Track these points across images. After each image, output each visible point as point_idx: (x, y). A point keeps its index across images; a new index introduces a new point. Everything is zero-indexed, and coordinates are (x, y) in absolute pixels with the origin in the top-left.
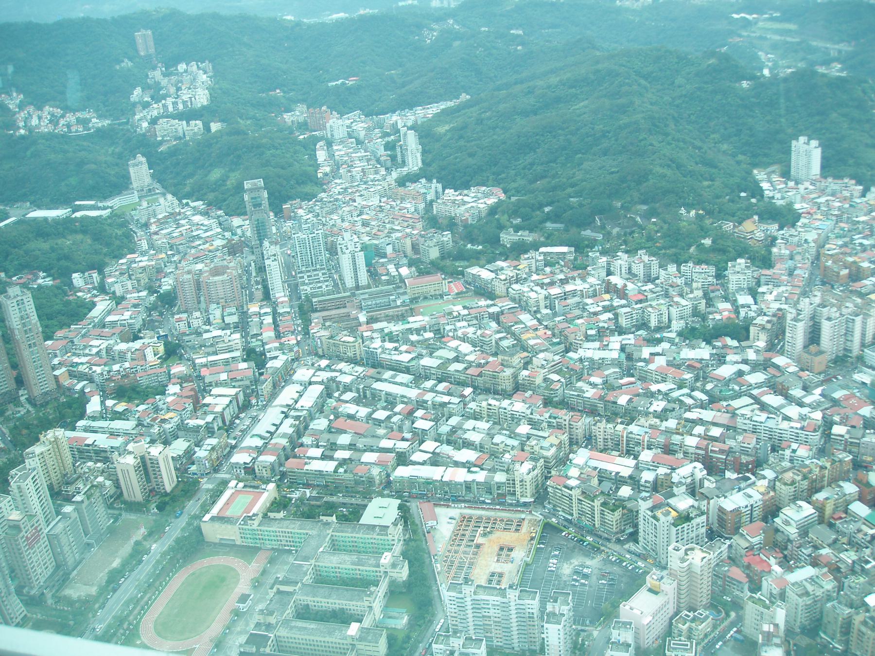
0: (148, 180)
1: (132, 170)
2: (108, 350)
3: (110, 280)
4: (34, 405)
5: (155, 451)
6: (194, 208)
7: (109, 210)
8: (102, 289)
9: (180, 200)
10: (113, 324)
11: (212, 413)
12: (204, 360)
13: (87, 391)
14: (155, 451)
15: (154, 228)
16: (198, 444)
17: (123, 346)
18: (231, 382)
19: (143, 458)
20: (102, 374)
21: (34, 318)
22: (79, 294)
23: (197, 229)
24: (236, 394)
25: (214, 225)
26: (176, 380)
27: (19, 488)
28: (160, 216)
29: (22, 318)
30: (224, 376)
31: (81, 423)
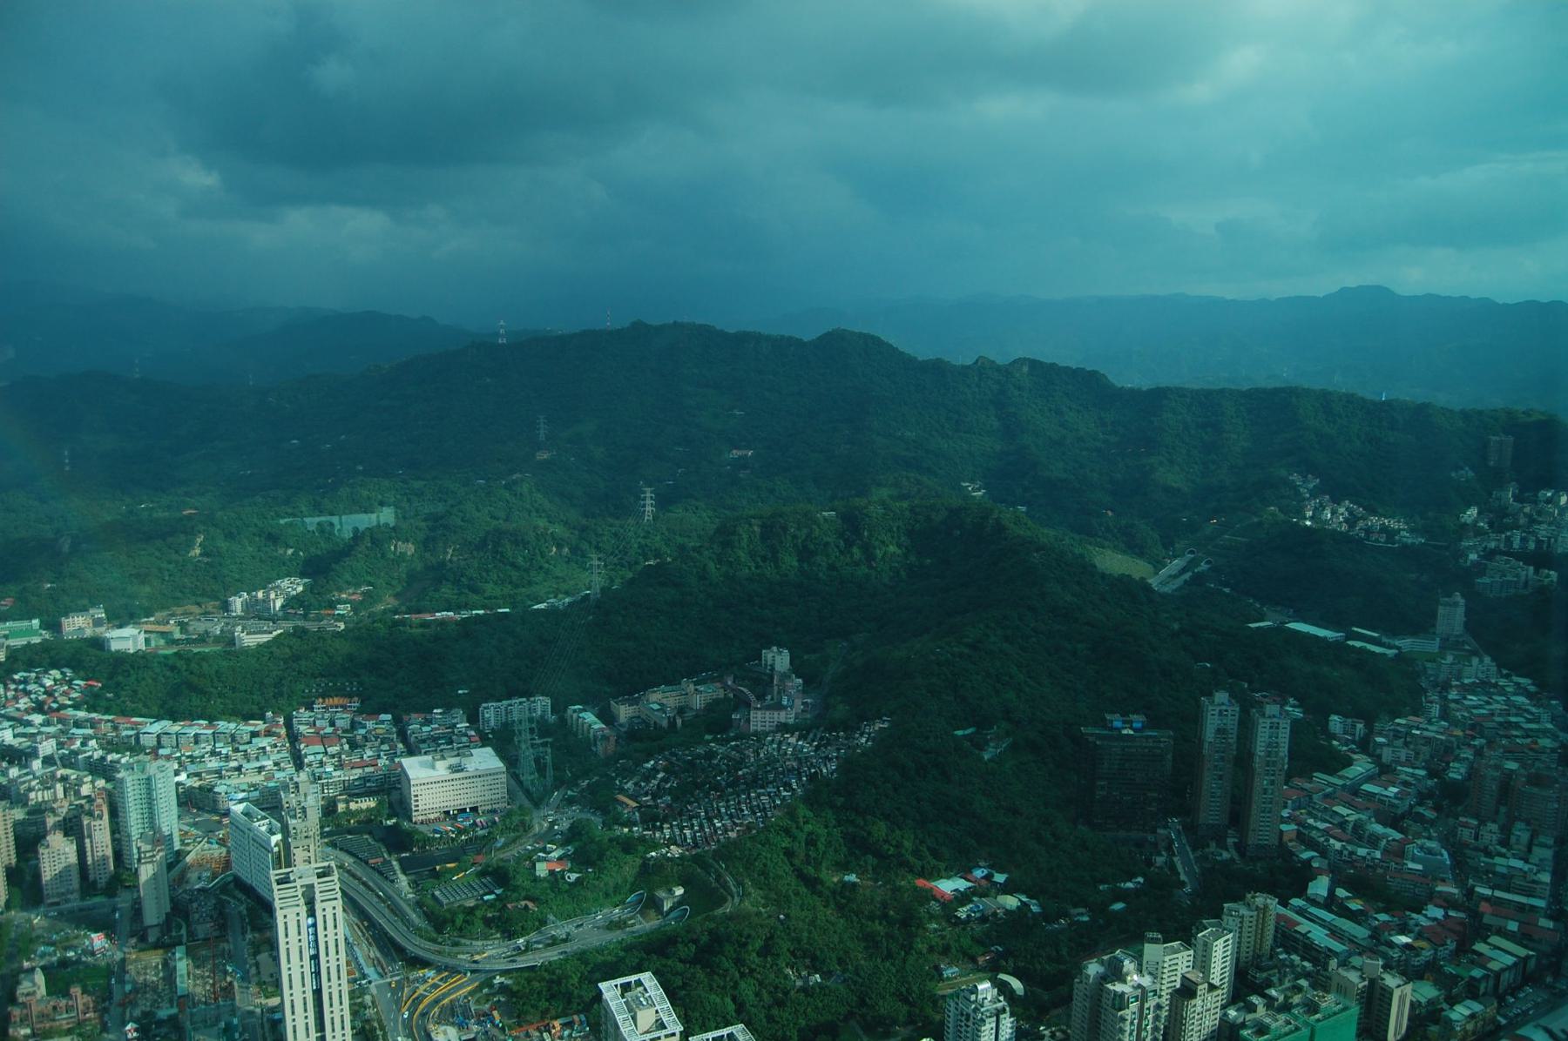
0: (1458, 628)
1: (1441, 610)
2: (1358, 826)
3: (1380, 740)
4: (1242, 854)
5: (1391, 981)
6: (1518, 684)
7: (1395, 651)
8: (1365, 746)
9: (1499, 667)
10: (1370, 796)
11: (1484, 967)
12: (1488, 892)
13: (1315, 865)
14: (1391, 981)
15: (1453, 695)
16: (1452, 1001)
17: (1378, 829)
18: (1521, 938)
19: (1372, 982)
20: (1341, 852)
21: (1284, 750)
22: (1335, 743)
23: (1516, 715)
24: (1528, 957)
25: (1545, 717)
26: (1439, 901)
27: (1206, 944)
28: (1466, 681)
29: (1269, 745)
30: (1513, 926)
31: (1297, 902)
